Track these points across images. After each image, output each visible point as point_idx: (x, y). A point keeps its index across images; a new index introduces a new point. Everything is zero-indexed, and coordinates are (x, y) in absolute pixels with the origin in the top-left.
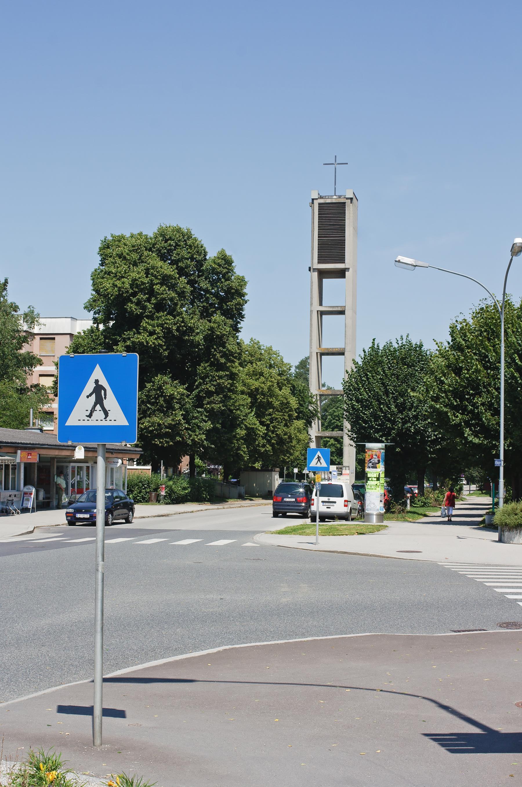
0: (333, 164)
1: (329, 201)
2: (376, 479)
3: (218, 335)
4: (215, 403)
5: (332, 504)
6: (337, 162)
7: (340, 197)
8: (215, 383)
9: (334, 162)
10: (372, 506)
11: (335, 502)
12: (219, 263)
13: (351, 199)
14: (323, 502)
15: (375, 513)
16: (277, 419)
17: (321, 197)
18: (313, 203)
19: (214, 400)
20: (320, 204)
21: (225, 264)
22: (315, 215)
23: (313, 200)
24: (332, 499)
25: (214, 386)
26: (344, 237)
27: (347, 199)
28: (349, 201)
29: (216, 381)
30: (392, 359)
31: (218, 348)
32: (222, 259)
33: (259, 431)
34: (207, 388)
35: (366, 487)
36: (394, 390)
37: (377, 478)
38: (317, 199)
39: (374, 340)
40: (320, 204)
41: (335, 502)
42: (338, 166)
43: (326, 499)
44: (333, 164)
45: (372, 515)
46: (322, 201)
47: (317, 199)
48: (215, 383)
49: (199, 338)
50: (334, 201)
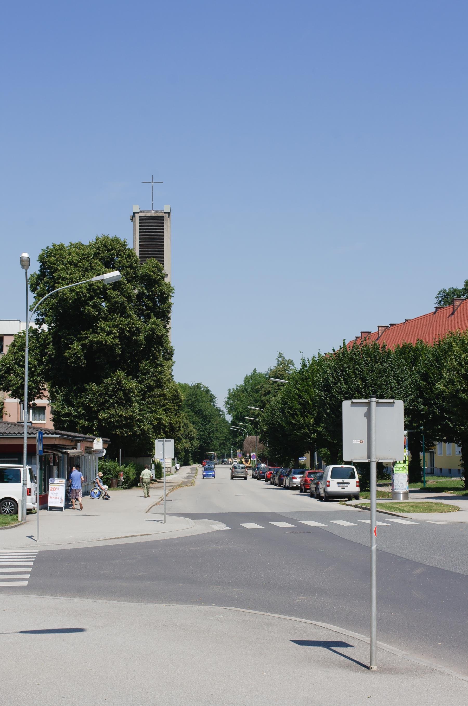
0: (150, 183)
1: (148, 215)
2: (403, 462)
3: (159, 335)
4: (155, 397)
5: (346, 485)
6: (154, 181)
7: (157, 212)
8: (155, 378)
9: (151, 181)
10: (401, 485)
11: (349, 483)
12: (153, 271)
13: (169, 214)
14: (338, 483)
15: (402, 491)
16: (170, 409)
17: (141, 212)
18: (134, 216)
19: (155, 393)
20: (140, 217)
21: (158, 272)
22: (136, 227)
23: (134, 213)
24: (346, 480)
25: (154, 381)
26: (163, 246)
27: (165, 213)
28: (167, 215)
29: (156, 376)
30: (366, 357)
31: (157, 347)
32: (155, 267)
33: (164, 420)
34: (148, 383)
35: (394, 469)
36: (373, 384)
37: (404, 461)
38: (138, 213)
39: (344, 340)
40: (140, 217)
41: (349, 483)
42: (154, 184)
43: (340, 480)
44: (150, 183)
45: (399, 493)
46: (142, 215)
47: (138, 213)
48: (155, 378)
49: (142, 337)
50: (153, 215)
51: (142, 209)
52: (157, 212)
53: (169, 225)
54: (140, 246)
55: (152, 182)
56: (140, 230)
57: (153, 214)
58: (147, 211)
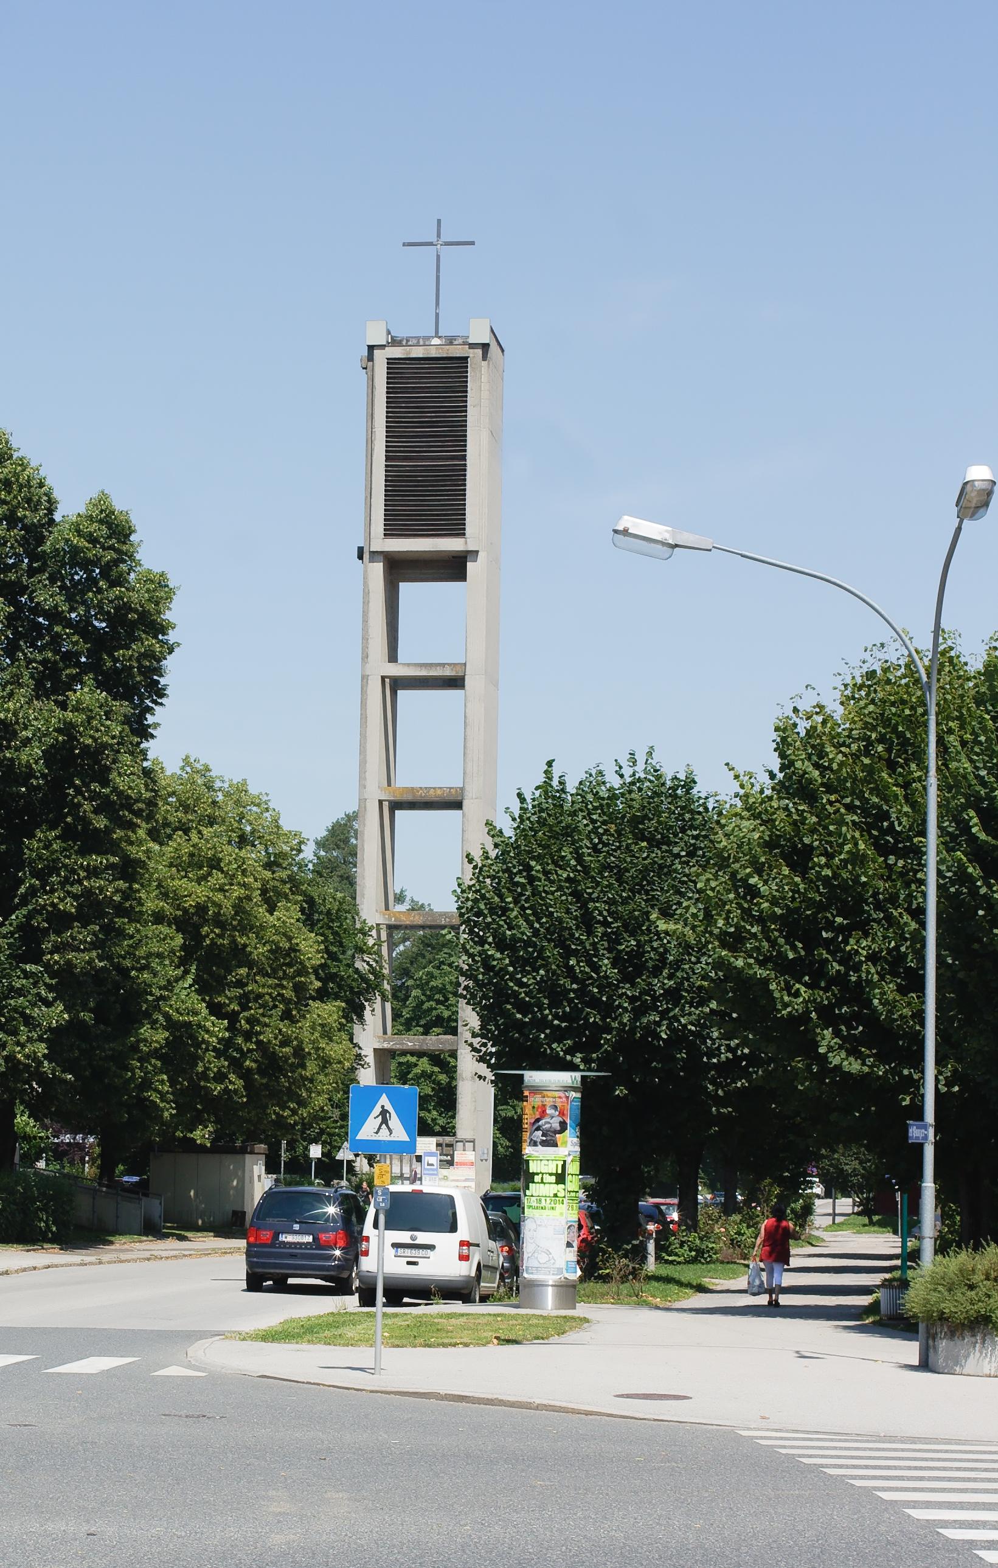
0: (431, 244)
1: (418, 352)
2: (553, 1179)
3: (88, 746)
4: (78, 950)
5: (422, 1252)
6: (443, 239)
7: (450, 341)
8: (76, 889)
9: (434, 239)
10: (543, 1258)
11: (432, 1247)
12: (91, 534)
13: (485, 347)
14: (396, 1246)
15: (551, 1279)
16: (260, 996)
17: (395, 342)
18: (371, 358)
19: (74, 938)
20: (391, 362)
21: (110, 537)
22: (376, 393)
23: (371, 348)
24: (423, 1237)
25: (75, 897)
26: (464, 458)
27: (473, 346)
28: (479, 352)
29: (79, 882)
30: (604, 823)
31: (87, 786)
32: (101, 522)
33: (207, 1031)
34: (53, 905)
35: (525, 1201)
36: (610, 914)
37: (556, 1174)
38: (382, 347)
39: (550, 764)
40: (391, 362)
41: (432, 1247)
42: (445, 251)
43: (404, 1237)
44: (431, 244)
45: (541, 1285)
46: (397, 352)
47: (382, 347)
48: (76, 889)
49: (31, 755)
50: (433, 353)
51: (398, 333)
52: (451, 343)
53: (485, 387)
54: (388, 458)
55: (438, 242)
56: (389, 402)
57: (435, 348)
58: (418, 338)
